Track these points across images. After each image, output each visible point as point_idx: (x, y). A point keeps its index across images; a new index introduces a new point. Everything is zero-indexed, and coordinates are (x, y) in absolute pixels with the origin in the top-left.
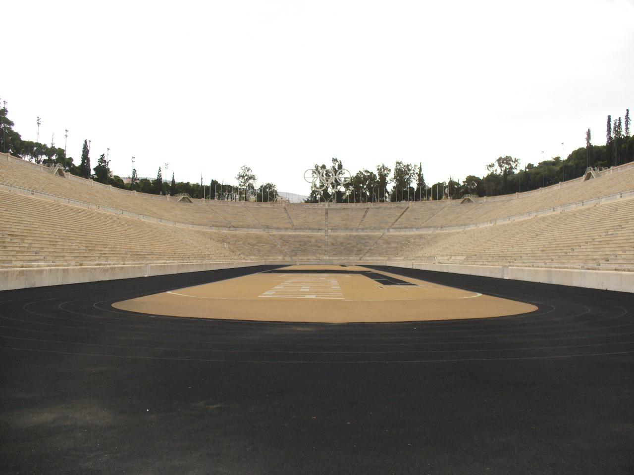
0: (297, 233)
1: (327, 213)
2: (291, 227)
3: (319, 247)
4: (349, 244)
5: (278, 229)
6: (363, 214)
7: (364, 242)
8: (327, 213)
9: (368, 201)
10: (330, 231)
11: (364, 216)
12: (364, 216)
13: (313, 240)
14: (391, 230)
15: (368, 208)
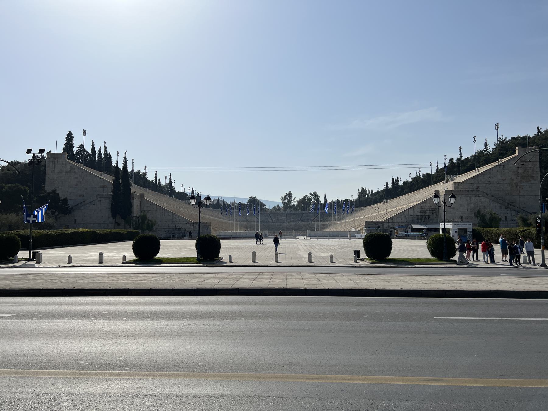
0: (275, 224)
1: (286, 216)
2: (272, 221)
3: (284, 230)
4: (295, 228)
5: (267, 222)
6: (301, 216)
7: (301, 227)
8: (286, 216)
9: (303, 210)
10: (287, 223)
11: (302, 217)
12: (302, 217)
13: (281, 227)
14: (312, 223)
15: (303, 213)
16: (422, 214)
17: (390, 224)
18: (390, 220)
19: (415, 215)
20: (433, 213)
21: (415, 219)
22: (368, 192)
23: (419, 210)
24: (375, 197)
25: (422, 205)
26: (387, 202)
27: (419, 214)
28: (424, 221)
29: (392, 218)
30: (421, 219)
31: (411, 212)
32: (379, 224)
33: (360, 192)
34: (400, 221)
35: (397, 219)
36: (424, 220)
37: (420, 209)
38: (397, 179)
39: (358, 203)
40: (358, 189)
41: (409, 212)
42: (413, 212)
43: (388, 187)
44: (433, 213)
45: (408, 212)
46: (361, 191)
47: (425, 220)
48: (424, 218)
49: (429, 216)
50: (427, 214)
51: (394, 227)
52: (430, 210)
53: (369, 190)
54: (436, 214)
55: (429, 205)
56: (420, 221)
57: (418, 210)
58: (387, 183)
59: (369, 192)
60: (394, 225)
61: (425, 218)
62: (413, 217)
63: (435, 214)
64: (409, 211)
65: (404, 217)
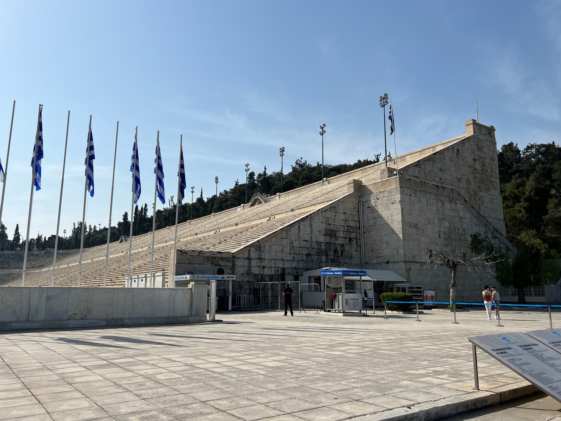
16: (328, 239)
17: (254, 263)
18: (252, 249)
19: (314, 240)
20: (350, 239)
21: (315, 253)
22: (88, 230)
23: (323, 227)
24: (103, 235)
25: (329, 214)
26: (126, 241)
27: (322, 239)
28: (332, 260)
29: (258, 246)
30: (327, 255)
31: (305, 231)
32: (222, 263)
33: (76, 227)
34: (279, 255)
35: (270, 247)
36: (332, 257)
37: (324, 224)
38: (144, 207)
39: (73, 242)
40: (74, 224)
41: (301, 232)
42: (308, 230)
43: (127, 219)
44: (350, 239)
45: (299, 231)
46: (78, 227)
47: (334, 256)
48: (332, 251)
49: (343, 245)
50: (340, 241)
51: (262, 275)
52: (346, 230)
53: (90, 226)
54: (357, 242)
55: (342, 216)
56: (324, 258)
57: (319, 226)
58: (126, 213)
59: (90, 229)
60: (264, 267)
61: (336, 251)
62: (308, 245)
63: (354, 241)
64: (301, 227)
65: (288, 245)
